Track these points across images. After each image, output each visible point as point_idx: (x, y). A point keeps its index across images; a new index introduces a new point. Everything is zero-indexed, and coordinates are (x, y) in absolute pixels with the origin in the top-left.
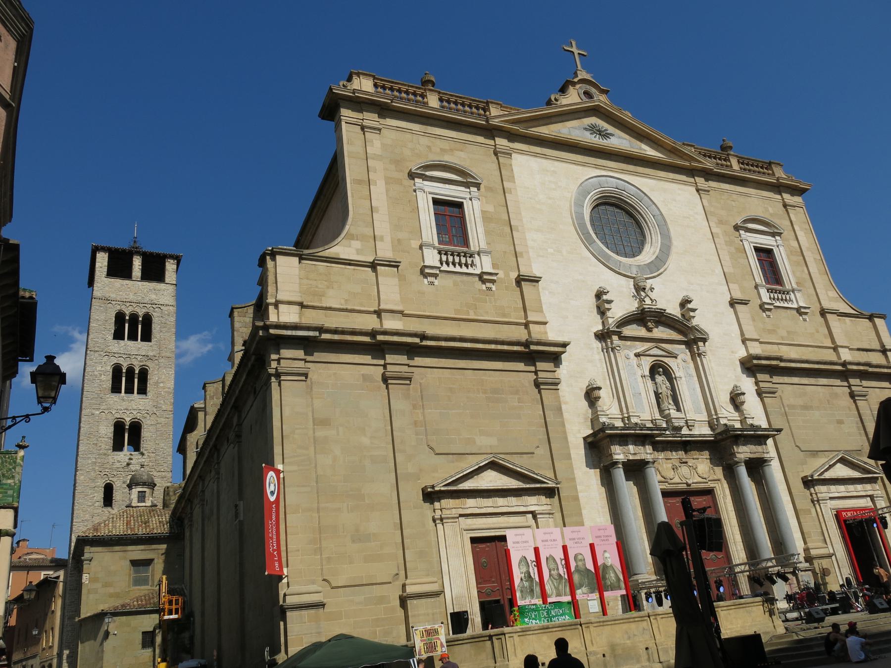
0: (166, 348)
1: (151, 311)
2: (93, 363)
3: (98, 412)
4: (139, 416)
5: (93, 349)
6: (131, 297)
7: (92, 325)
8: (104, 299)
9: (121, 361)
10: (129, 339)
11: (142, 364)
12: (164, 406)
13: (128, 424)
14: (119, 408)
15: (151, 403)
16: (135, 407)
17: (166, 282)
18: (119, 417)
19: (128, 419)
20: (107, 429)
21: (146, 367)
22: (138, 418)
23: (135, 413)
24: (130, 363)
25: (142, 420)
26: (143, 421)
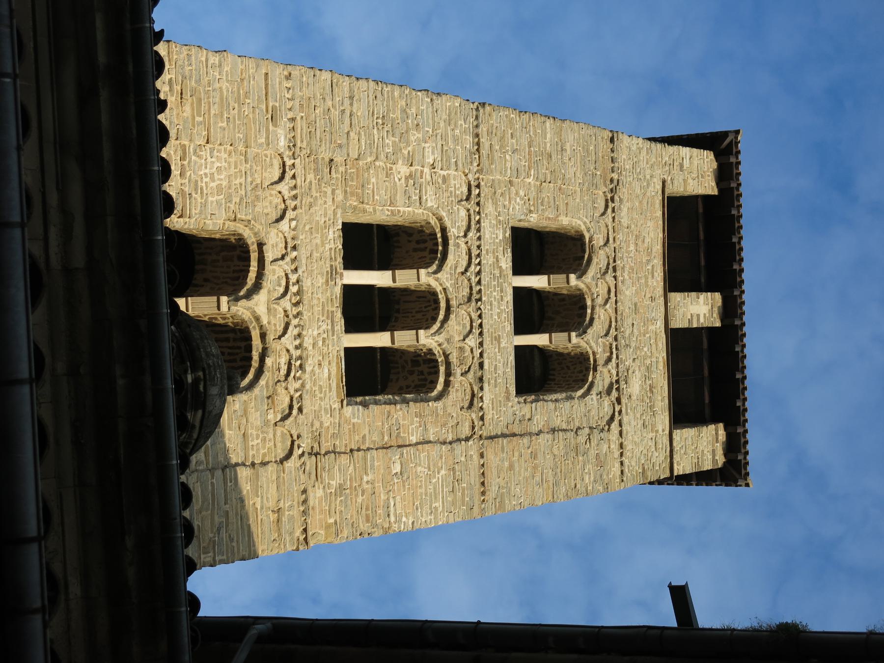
0: (511, 467)
1: (602, 378)
2: (442, 124)
3: (282, 143)
4: (276, 361)
5: (483, 129)
6: (628, 292)
7: (548, 124)
8: (612, 180)
9: (456, 257)
10: (520, 293)
11: (453, 359)
12: (320, 493)
13: (242, 310)
14: (303, 253)
15: (327, 421)
16: (308, 342)
17: (678, 434)
18: (269, 256)
19: (260, 303)
20: (219, 188)
21: (441, 379)
22: (269, 361)
23: (288, 341)
24: (453, 303)
25: (262, 382)
26: (257, 390)
